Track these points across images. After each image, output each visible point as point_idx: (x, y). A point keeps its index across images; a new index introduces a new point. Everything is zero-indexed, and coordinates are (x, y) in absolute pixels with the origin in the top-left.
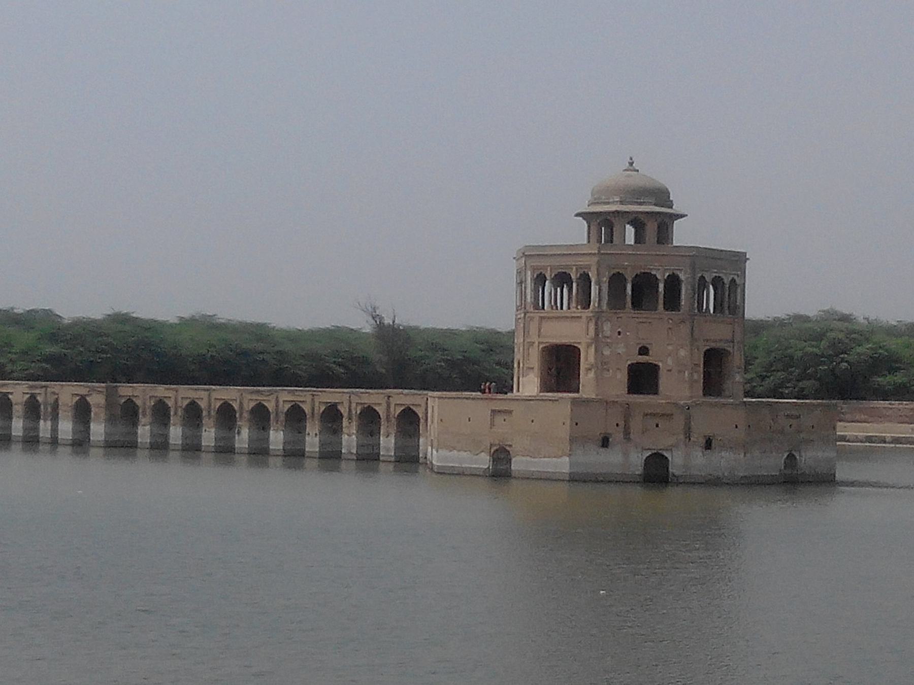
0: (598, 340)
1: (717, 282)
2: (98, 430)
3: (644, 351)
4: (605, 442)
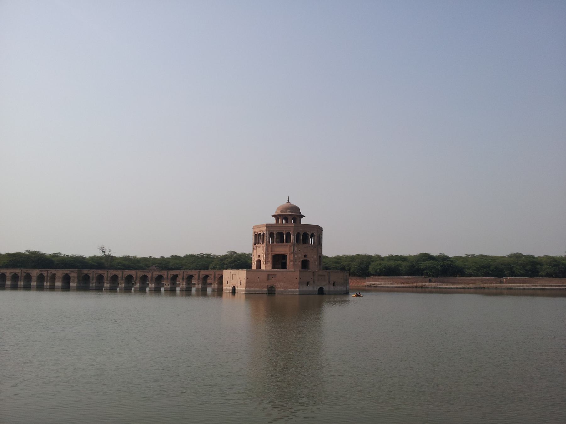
0: (294, 253)
3: (305, 256)
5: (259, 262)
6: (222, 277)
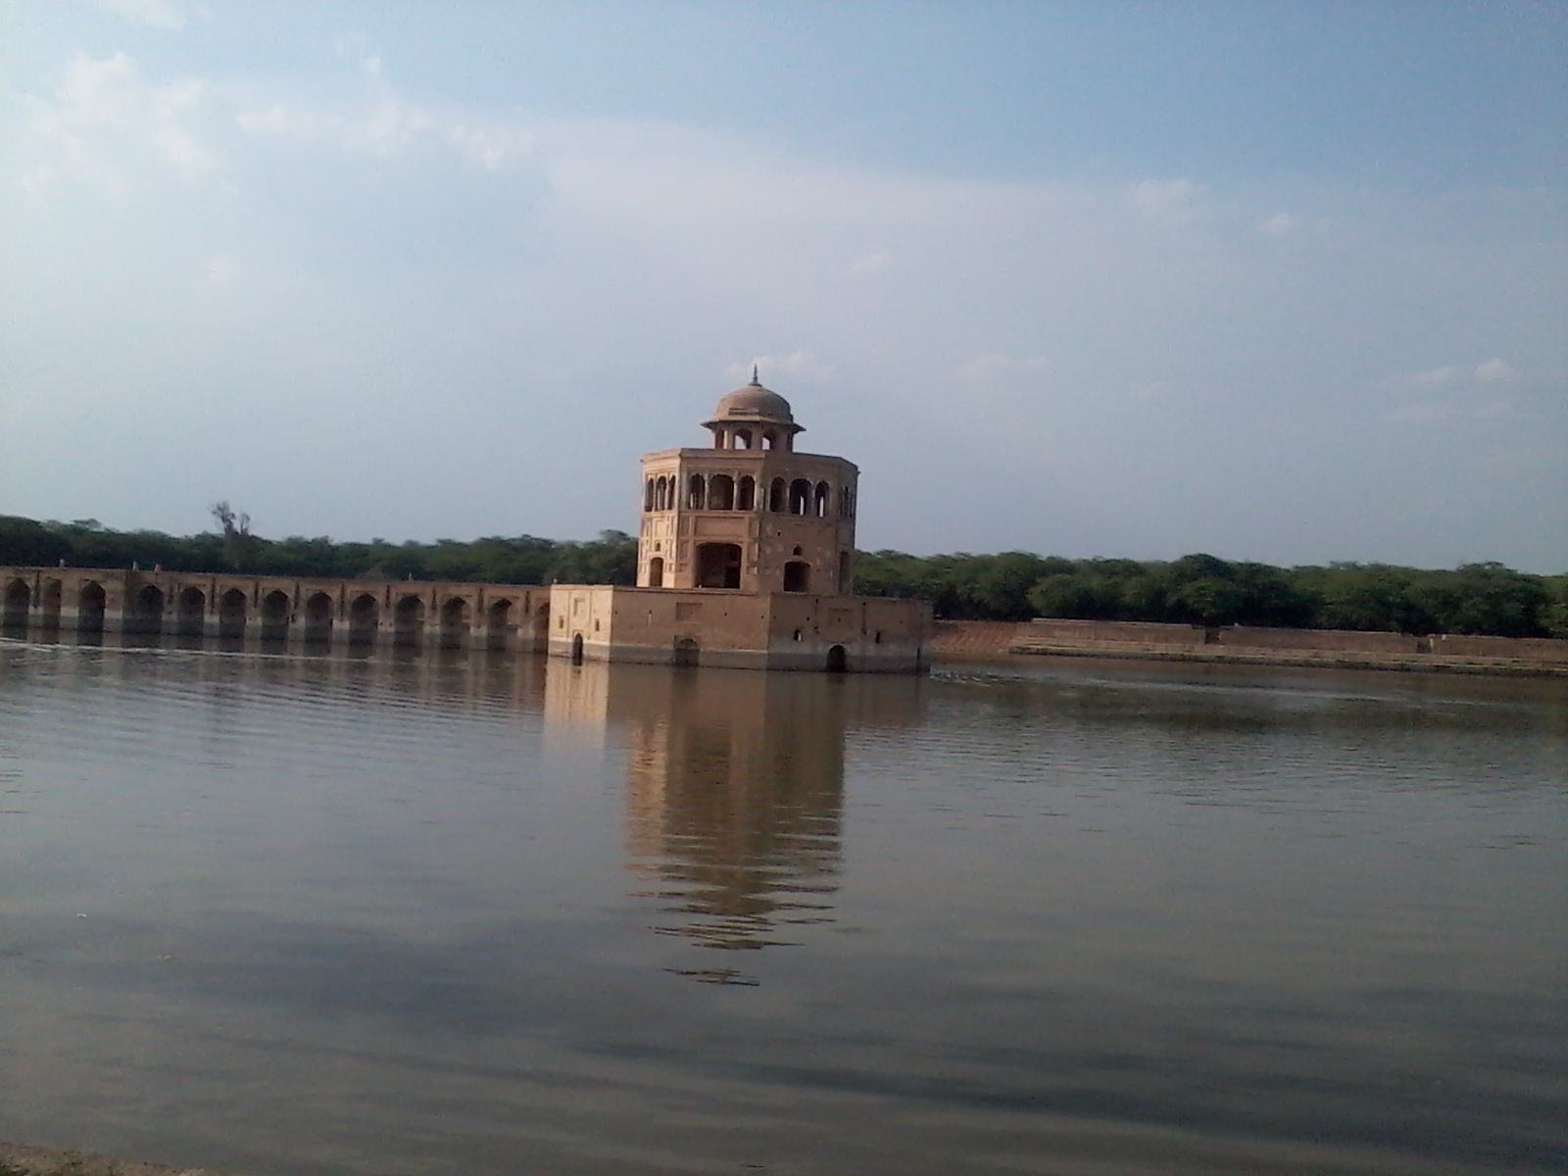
2: (113, 615)
3: (797, 551)
5: (658, 564)
6: (545, 608)
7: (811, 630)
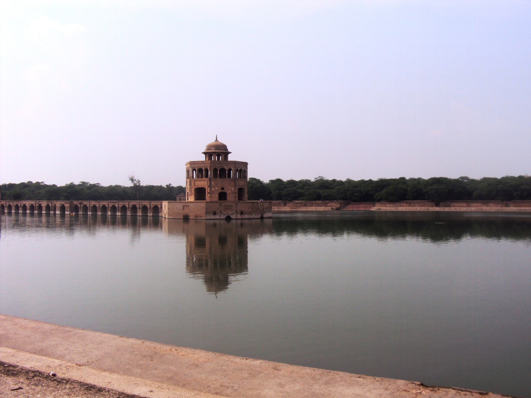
1: (241, 170)
3: (223, 189)
4: (215, 214)
7: (219, 212)
